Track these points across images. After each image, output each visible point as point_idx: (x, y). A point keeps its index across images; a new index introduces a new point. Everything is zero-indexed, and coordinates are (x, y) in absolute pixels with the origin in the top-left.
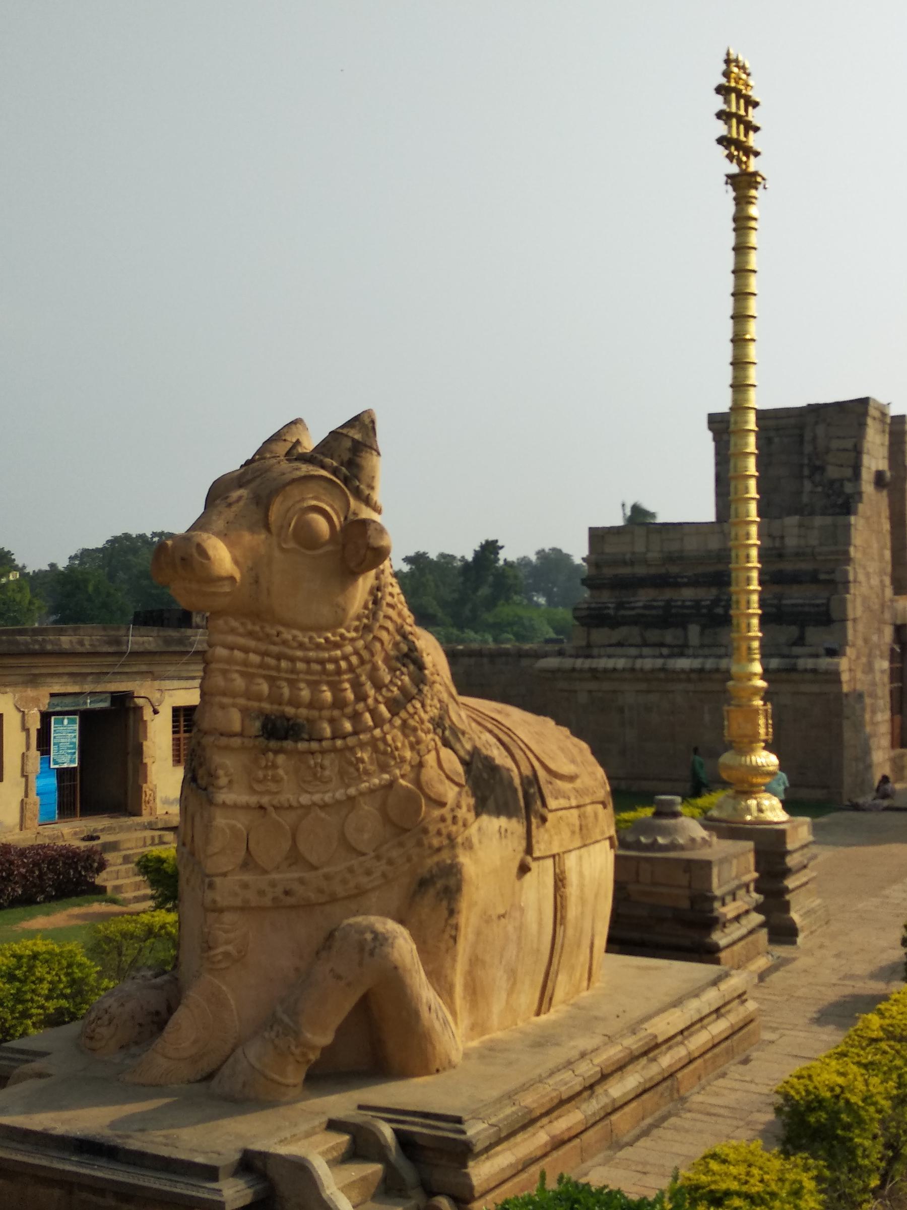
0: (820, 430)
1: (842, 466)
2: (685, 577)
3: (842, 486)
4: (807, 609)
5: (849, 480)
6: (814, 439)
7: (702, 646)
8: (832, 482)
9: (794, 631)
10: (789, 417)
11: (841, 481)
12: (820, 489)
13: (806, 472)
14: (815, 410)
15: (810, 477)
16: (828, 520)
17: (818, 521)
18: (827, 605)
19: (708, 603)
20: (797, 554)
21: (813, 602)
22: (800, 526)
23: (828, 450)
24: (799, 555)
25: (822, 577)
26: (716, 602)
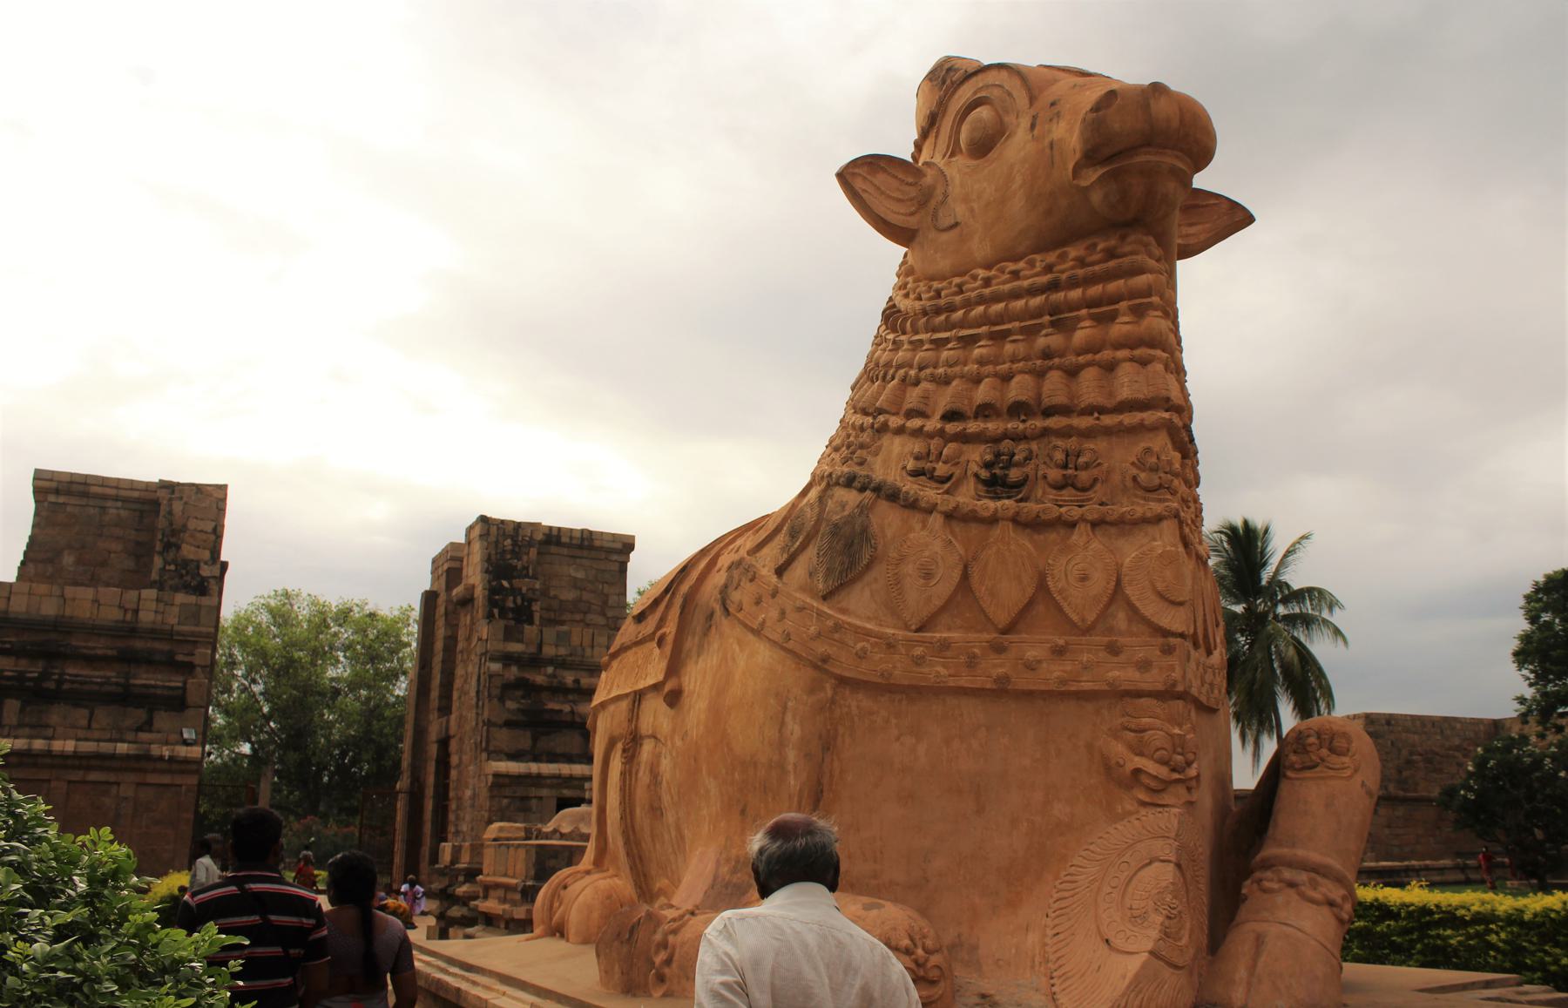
0: (177, 507)
1: (198, 547)
2: (10, 642)
3: (198, 567)
4: (159, 692)
5: (206, 563)
6: (170, 513)
7: (20, 725)
8: (186, 563)
9: (140, 715)
10: (132, 489)
11: (198, 562)
12: (172, 567)
13: (158, 547)
14: (169, 487)
15: (161, 553)
16: (192, 599)
17: (180, 598)
18: (184, 689)
19: (36, 675)
20: (153, 631)
21: (167, 684)
22: (158, 600)
23: (184, 528)
24: (154, 633)
25: (180, 658)
26: (45, 676)
